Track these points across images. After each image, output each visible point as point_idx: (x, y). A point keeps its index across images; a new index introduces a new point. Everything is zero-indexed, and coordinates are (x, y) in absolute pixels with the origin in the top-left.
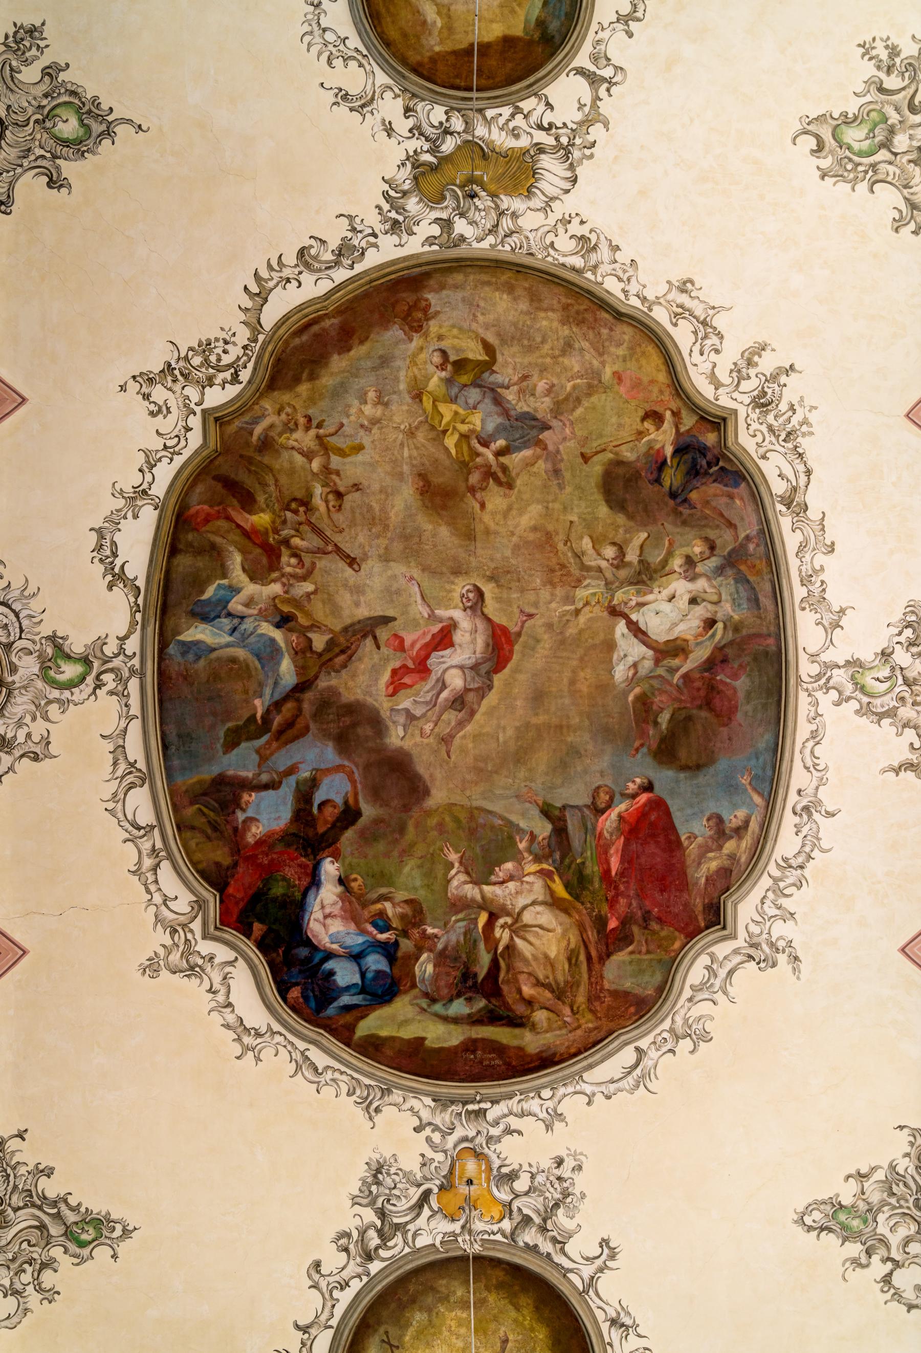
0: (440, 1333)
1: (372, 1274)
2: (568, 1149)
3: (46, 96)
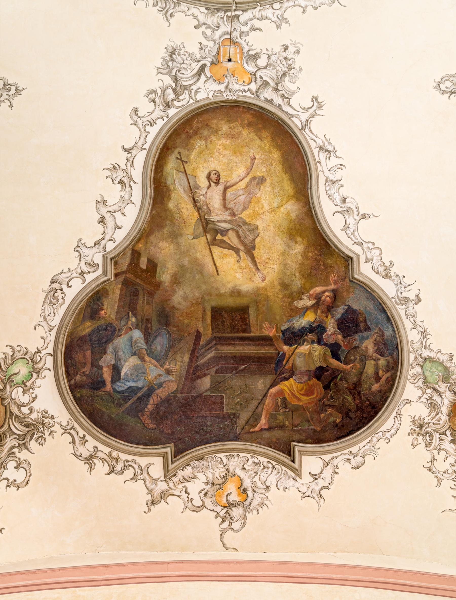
0: (213, 153)
1: (170, 116)
2: (291, 40)
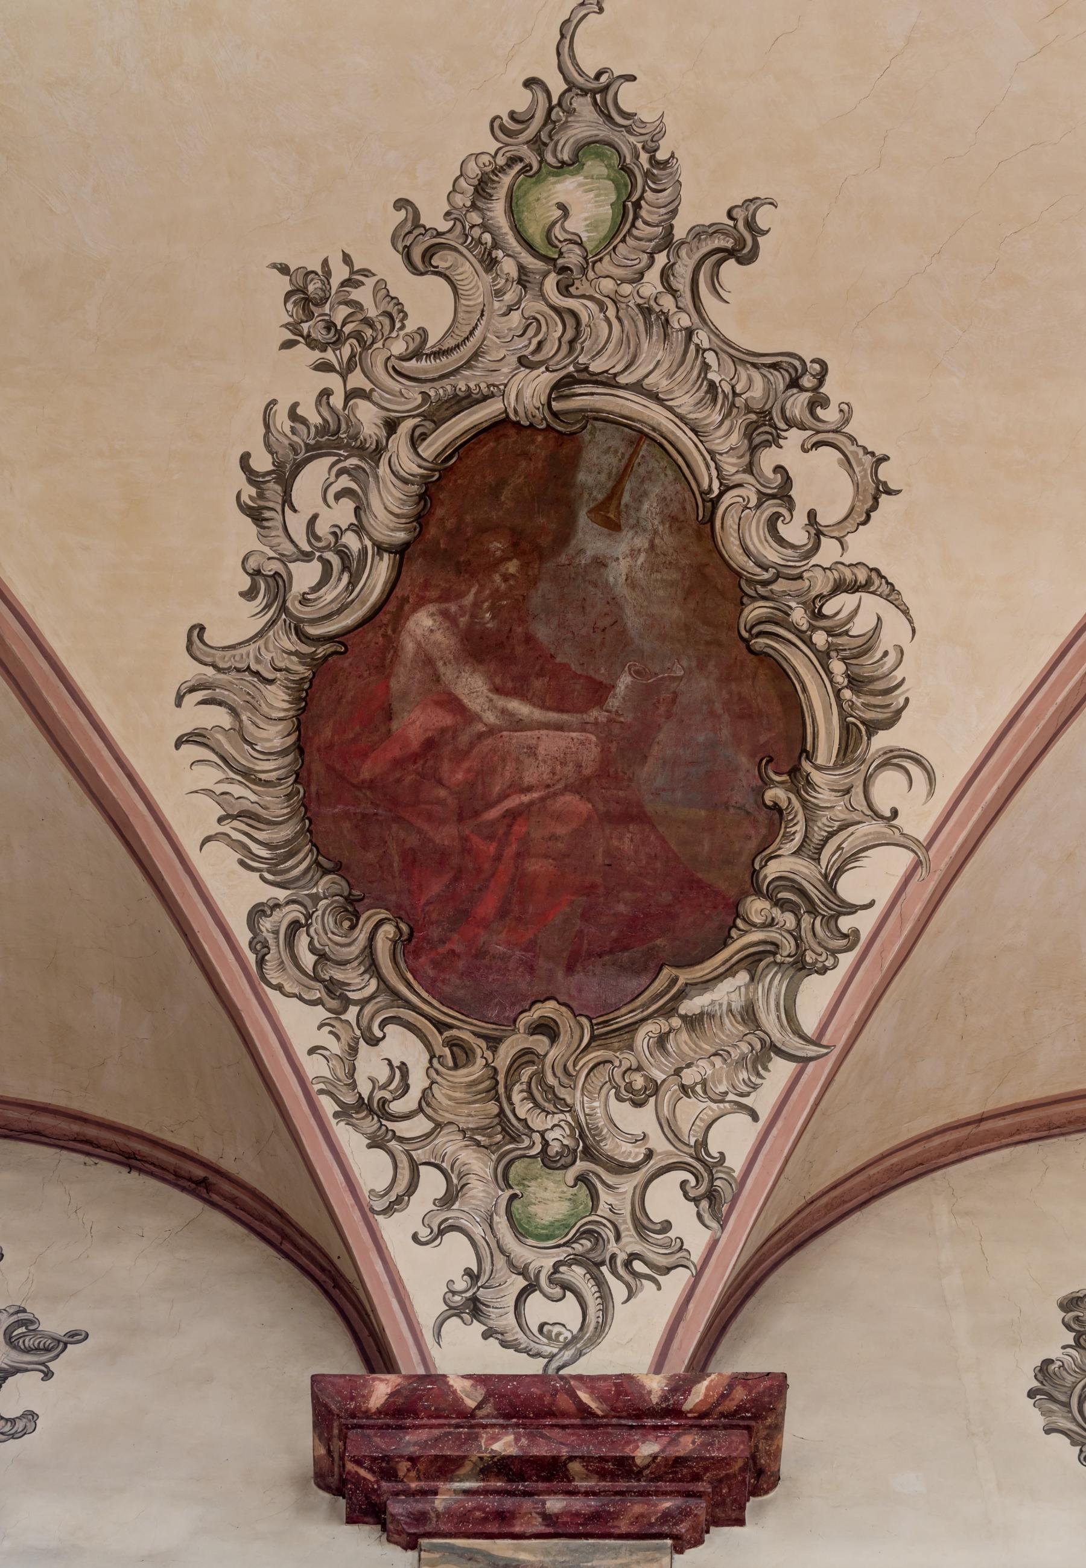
3: (490, 264)
